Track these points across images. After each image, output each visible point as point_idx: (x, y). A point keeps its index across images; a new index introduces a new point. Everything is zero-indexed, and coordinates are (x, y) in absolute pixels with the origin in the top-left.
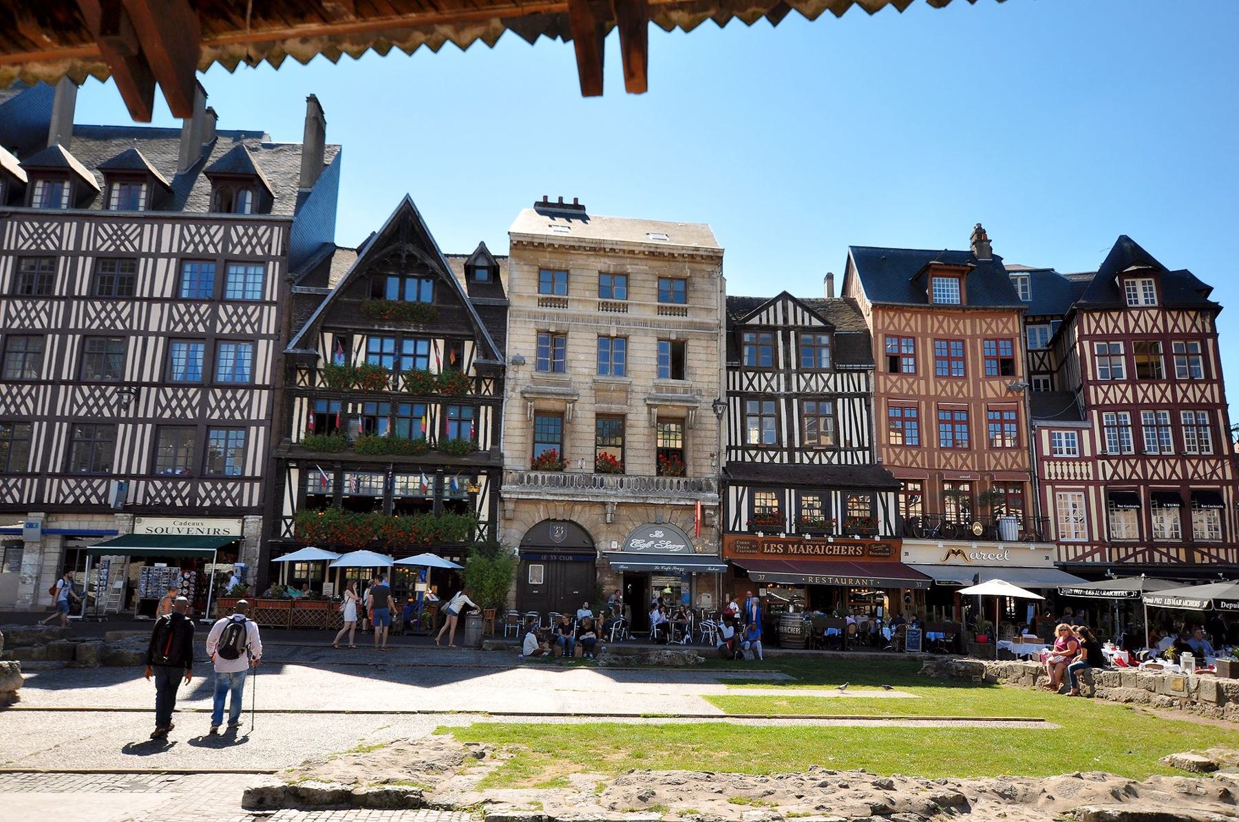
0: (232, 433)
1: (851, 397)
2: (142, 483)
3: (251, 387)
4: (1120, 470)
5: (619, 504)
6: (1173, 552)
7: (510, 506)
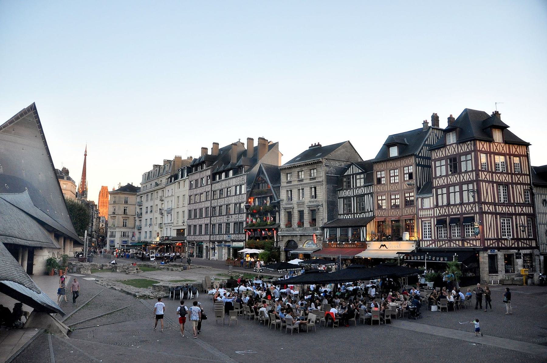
1: (368, 194)
4: (441, 212)
5: (300, 236)
6: (457, 242)
7: (280, 237)
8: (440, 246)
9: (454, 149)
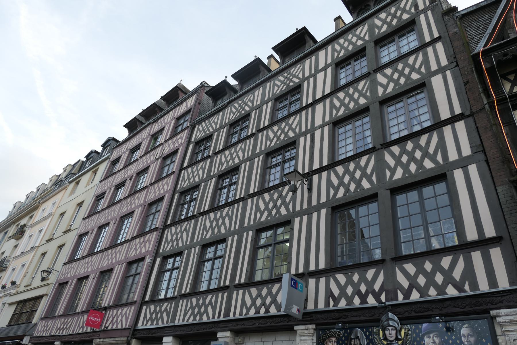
0: (428, 191)
2: (323, 280)
3: (438, 125)
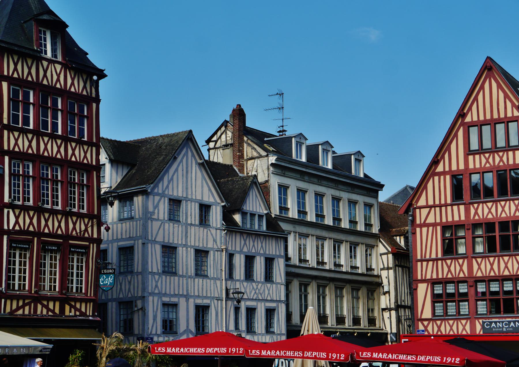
8: (12, 312)
9: (58, 76)
